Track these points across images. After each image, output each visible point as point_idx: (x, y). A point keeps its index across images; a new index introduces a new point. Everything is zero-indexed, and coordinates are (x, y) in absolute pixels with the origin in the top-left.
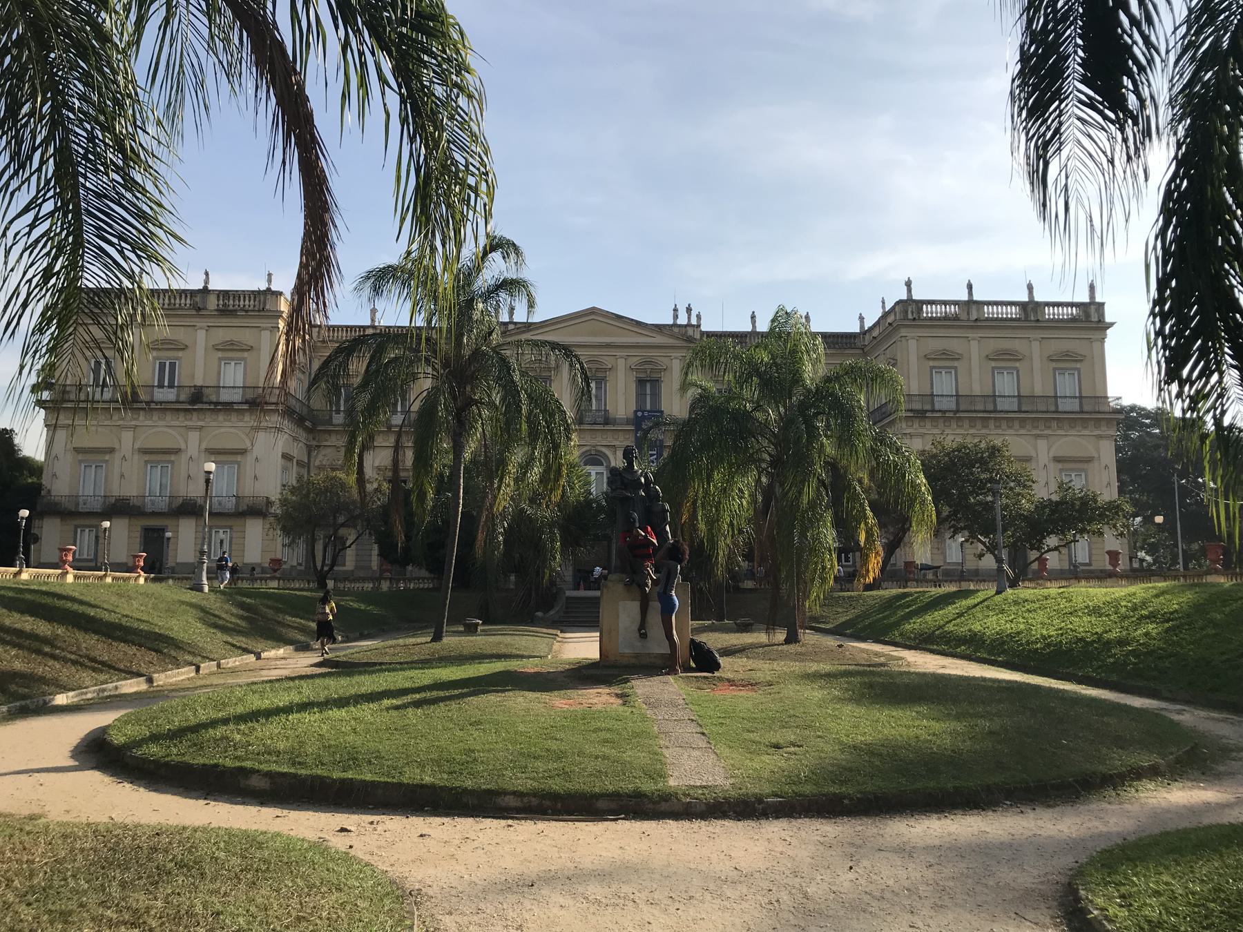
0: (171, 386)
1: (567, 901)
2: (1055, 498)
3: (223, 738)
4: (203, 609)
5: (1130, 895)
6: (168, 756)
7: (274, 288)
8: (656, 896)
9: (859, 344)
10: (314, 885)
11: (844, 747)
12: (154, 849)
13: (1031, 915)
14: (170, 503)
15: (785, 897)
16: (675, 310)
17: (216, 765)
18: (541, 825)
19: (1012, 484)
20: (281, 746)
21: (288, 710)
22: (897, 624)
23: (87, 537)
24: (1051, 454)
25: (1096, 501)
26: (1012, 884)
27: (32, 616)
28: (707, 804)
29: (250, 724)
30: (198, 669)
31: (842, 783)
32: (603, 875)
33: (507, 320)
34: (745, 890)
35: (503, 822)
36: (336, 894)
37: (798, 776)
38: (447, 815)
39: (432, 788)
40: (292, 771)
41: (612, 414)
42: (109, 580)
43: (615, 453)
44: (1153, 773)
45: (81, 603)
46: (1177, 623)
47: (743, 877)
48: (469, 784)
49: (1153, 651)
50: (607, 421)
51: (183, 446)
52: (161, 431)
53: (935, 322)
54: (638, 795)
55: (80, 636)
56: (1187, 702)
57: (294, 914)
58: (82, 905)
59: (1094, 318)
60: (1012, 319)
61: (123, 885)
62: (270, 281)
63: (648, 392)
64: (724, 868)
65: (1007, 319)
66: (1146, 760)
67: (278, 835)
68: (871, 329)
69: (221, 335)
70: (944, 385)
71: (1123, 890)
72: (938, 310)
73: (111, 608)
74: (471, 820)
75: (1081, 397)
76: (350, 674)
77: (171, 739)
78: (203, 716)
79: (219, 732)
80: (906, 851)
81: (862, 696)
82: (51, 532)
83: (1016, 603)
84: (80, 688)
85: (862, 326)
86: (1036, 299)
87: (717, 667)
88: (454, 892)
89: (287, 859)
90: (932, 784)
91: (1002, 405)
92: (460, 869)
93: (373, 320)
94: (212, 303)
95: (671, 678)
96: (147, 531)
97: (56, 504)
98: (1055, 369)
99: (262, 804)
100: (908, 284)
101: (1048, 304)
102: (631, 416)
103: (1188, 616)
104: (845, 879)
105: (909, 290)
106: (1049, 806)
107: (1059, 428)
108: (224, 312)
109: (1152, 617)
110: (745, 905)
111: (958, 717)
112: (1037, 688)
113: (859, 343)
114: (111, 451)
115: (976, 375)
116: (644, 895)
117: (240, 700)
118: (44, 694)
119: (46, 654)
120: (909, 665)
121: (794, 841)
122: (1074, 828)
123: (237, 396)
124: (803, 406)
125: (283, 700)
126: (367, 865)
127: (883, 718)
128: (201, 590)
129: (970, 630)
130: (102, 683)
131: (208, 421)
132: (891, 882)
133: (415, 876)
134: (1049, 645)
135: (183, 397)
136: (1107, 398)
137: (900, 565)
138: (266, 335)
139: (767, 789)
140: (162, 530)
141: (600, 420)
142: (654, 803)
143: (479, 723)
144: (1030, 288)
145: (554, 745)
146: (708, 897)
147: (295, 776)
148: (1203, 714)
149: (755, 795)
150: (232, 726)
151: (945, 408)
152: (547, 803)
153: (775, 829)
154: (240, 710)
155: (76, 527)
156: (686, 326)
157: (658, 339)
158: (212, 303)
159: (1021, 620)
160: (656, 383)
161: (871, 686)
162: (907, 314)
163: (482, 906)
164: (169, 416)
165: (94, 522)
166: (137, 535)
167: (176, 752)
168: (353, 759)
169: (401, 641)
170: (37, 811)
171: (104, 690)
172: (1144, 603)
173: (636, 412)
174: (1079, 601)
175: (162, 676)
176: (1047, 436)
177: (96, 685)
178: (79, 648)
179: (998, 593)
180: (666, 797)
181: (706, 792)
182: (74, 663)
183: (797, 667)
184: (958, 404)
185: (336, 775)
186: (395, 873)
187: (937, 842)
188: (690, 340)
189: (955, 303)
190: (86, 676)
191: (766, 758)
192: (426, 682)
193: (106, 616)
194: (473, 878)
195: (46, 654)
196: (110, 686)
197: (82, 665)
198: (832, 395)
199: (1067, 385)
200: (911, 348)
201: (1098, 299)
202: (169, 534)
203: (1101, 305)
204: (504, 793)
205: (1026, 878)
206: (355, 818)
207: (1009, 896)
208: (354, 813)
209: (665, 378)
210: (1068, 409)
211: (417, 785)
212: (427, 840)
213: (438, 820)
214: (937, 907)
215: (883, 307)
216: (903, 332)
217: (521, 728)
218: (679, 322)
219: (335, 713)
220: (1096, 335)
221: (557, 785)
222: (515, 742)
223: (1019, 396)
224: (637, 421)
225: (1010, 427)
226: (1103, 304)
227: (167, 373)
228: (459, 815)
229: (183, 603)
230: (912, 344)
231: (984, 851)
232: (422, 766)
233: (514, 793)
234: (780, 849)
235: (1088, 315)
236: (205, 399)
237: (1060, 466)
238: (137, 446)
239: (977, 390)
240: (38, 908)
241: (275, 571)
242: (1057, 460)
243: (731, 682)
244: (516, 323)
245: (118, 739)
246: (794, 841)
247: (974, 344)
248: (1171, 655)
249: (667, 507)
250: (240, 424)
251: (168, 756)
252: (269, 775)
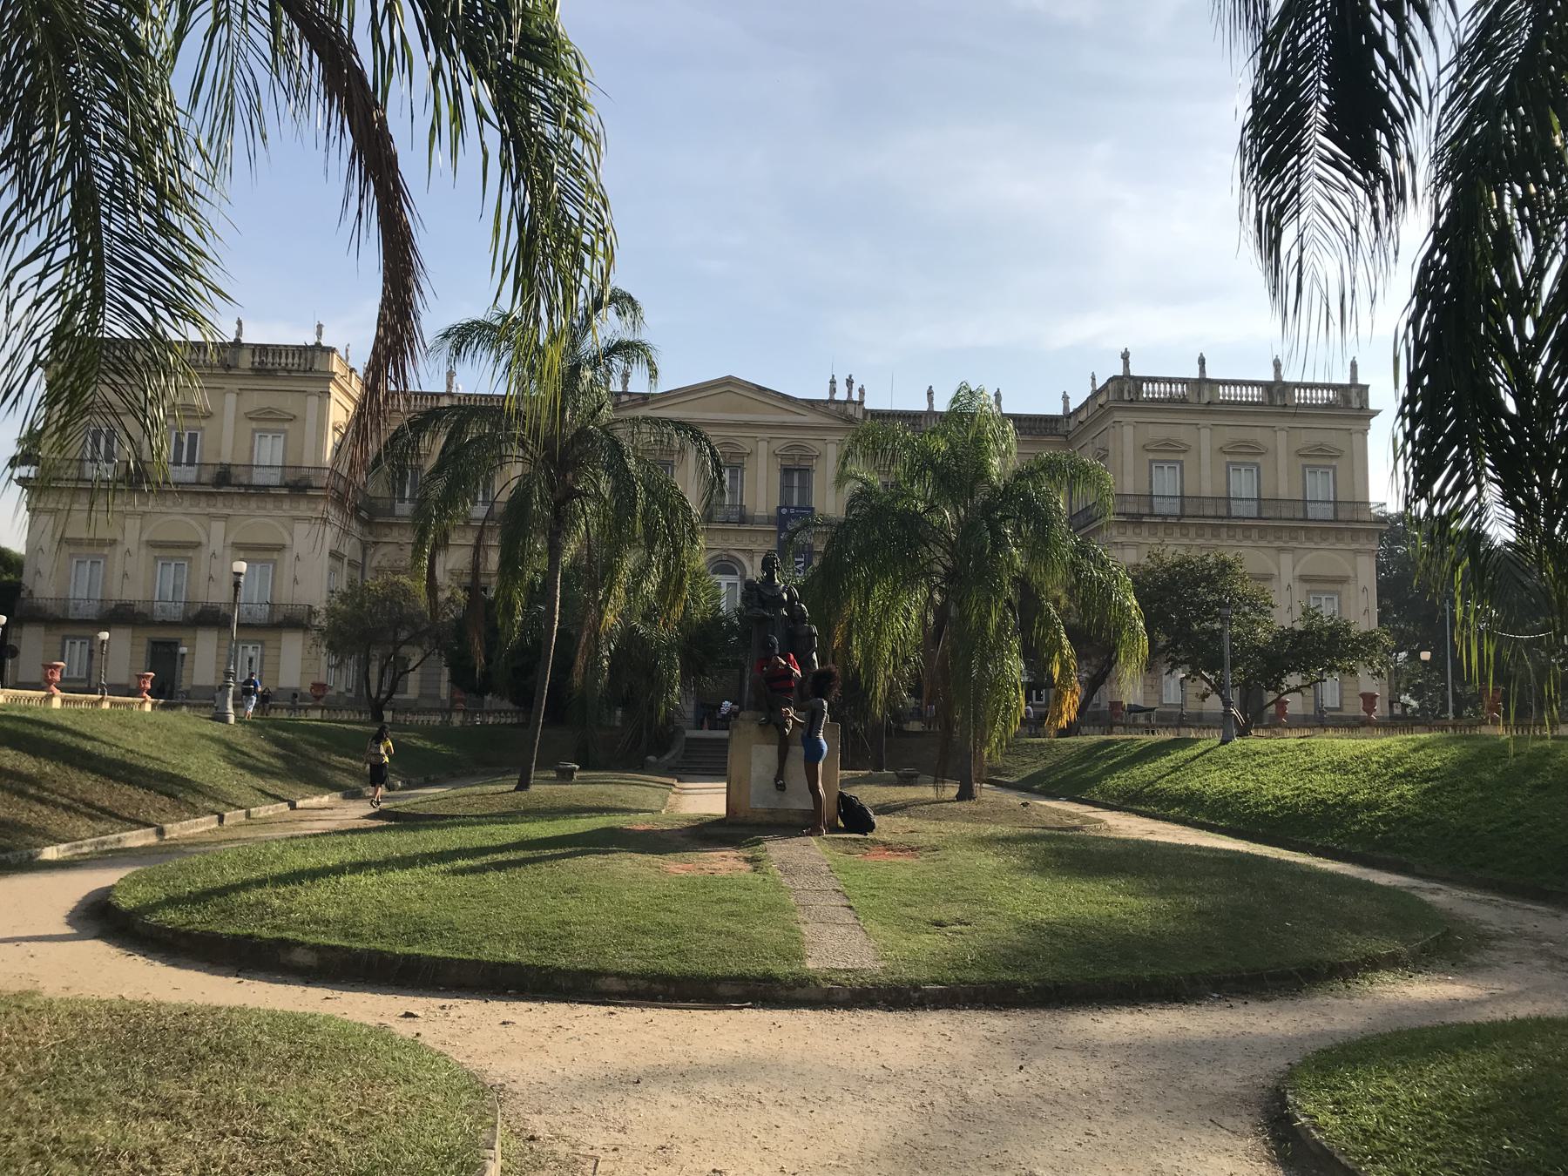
0: (191, 463)
1: (681, 1100)
2: (1299, 627)
3: (258, 903)
4: (228, 746)
5: (1346, 1101)
6: (189, 923)
7: (324, 343)
8: (787, 1096)
9: (1061, 430)
10: (378, 1076)
11: (1022, 927)
12: (184, 1031)
13: (1228, 1122)
14: (185, 612)
15: (940, 1099)
16: (833, 382)
17: (251, 936)
18: (650, 1013)
19: (1247, 609)
20: (331, 913)
21: (338, 870)
22: (1097, 779)
23: (77, 651)
24: (1298, 572)
25: (1348, 632)
26: (1211, 1088)
27: (13, 748)
28: (852, 991)
29: (291, 887)
30: (221, 819)
31: (1017, 968)
32: (723, 1072)
34: (893, 1091)
35: (604, 1009)
36: (404, 1087)
37: (964, 959)
38: (535, 1000)
39: (517, 966)
40: (345, 944)
41: (749, 510)
42: (106, 706)
43: (752, 559)
44: (1393, 963)
45: (75, 734)
46: (1438, 784)
47: (891, 1076)
48: (563, 962)
49: (1408, 817)
50: (743, 519)
51: (204, 540)
52: (177, 520)
53: (1156, 404)
54: (769, 979)
55: (74, 775)
56: (1444, 880)
57: (355, 1107)
58: (99, 1093)
59: (1356, 404)
60: (1252, 404)
61: (149, 1071)
62: (319, 334)
63: (796, 483)
64: (871, 1066)
65: (1247, 403)
66: (1383, 947)
67: (331, 1018)
68: (1077, 411)
69: (256, 401)
70: (1166, 483)
71: (1337, 1095)
72: (1161, 390)
73: (113, 741)
74: (564, 1006)
75: (1335, 502)
76: (415, 829)
77: (193, 903)
78: (232, 876)
79: (253, 896)
80: (1089, 1050)
81: (1048, 865)
82: (32, 644)
83: (1245, 755)
84: (74, 839)
85: (1066, 407)
86: (1286, 379)
87: (868, 826)
88: (543, 1088)
89: (344, 1046)
90: (1125, 972)
91: (1238, 509)
92: (551, 1062)
93: (449, 386)
94: (246, 360)
95: (813, 840)
96: (155, 645)
97: (39, 609)
98: (1304, 467)
99: (307, 983)
100: (1125, 357)
101: (1299, 385)
102: (773, 511)
103: (1452, 774)
104: (1013, 1081)
105: (1126, 364)
106: (1266, 1000)
107: (1309, 539)
108: (261, 372)
109: (1408, 776)
110: (892, 1108)
111: (1161, 893)
112: (1263, 859)
113: (1061, 429)
114: (113, 542)
115: (1206, 471)
116: (771, 1095)
117: (279, 857)
118: (29, 846)
119: (32, 797)
120: (1109, 829)
121: (955, 1037)
122: (1291, 1026)
123: (274, 478)
124: (988, 508)
125: (331, 859)
126: (440, 1054)
127: (1071, 893)
128: (225, 720)
129: (1187, 788)
130: (102, 834)
131: (238, 508)
132: (1067, 1085)
133: (497, 1070)
134: (1282, 808)
135: (205, 478)
136: (1368, 503)
137: (1105, 705)
138: (313, 401)
139: (925, 974)
140: (173, 645)
141: (735, 517)
142: (789, 989)
143: (575, 890)
144: (1277, 365)
145: (667, 918)
146: (848, 1097)
147: (348, 950)
148: (1464, 894)
149: (910, 981)
150: (269, 889)
151: (1165, 511)
152: (658, 987)
153: (932, 1022)
154: (278, 869)
155: (65, 638)
157: (810, 418)
158: (246, 360)
159: (1250, 777)
160: (805, 472)
161: (1058, 853)
162: (1123, 393)
163: (577, 1104)
164: (186, 503)
165: (88, 632)
166: (143, 650)
167: (200, 920)
168: (421, 931)
169: (477, 789)
170: (29, 987)
171: (104, 843)
172: (1399, 759)
173: (779, 508)
174: (1321, 756)
175: (177, 826)
176: (1293, 549)
177: (93, 836)
178: (72, 790)
179: (1224, 742)
180: (802, 982)
181: (851, 976)
182: (67, 808)
183: (969, 829)
184: (1182, 506)
185: (400, 949)
186: (473, 1065)
187: (1127, 1040)
188: (850, 420)
189: (1184, 381)
190: (82, 825)
191: (925, 938)
192: (510, 840)
193: (106, 751)
194: (567, 1073)
195: (32, 797)
196: (112, 837)
197: (76, 811)
198: (1024, 494)
199: (1319, 487)
200: (1127, 436)
201: (1361, 381)
202: (183, 650)
203: (1366, 387)
204: (604, 974)
205: (1231, 1080)
206: (422, 1001)
207: (1205, 1101)
208: (421, 995)
209: (817, 466)
210: (1320, 516)
211: (499, 964)
212: (510, 1028)
213: (525, 1005)
214: (1121, 1113)
215: (1093, 384)
216: (1117, 416)
217: (628, 896)
218: (837, 397)
219: (398, 876)
220: (1356, 426)
221: (670, 965)
222: (619, 914)
223: (1259, 499)
224: (781, 520)
225: (1248, 538)
226: (1366, 387)
227: (187, 450)
228: (551, 1000)
229: (202, 736)
230: (1128, 431)
231: (1182, 1050)
232: (505, 940)
233: (618, 974)
234: (937, 1045)
235: (1347, 401)
236: (233, 481)
237: (1308, 586)
238: (144, 538)
239: (1207, 491)
240: (48, 1096)
241: (318, 698)
242: (1304, 579)
243: (887, 846)
244: (630, 394)
245: (126, 902)
246: (955, 1037)
247: (1205, 433)
248: (1428, 823)
249: (815, 630)
250: (275, 513)
251: (189, 923)
252: (316, 948)
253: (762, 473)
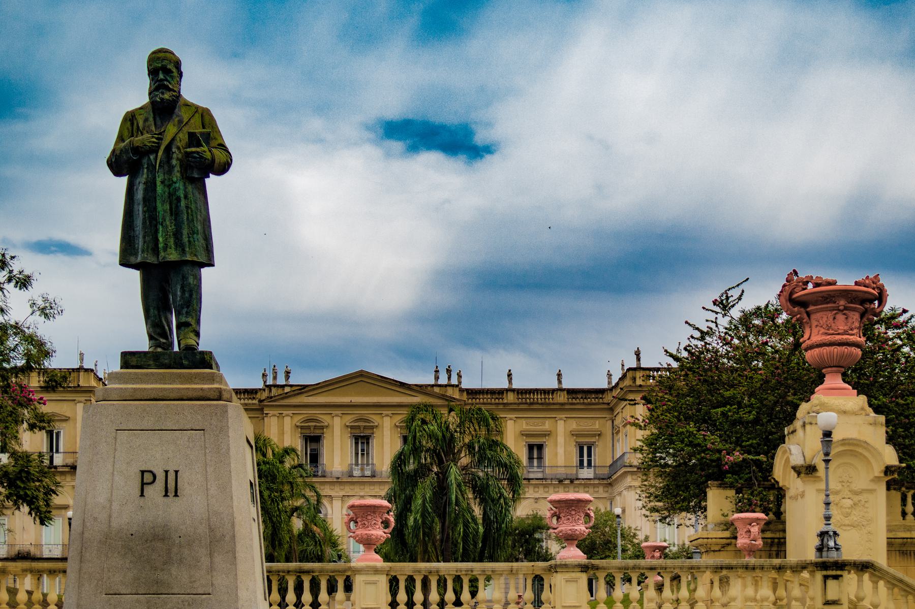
33: (284, 383)
62: (82, 360)
85: (609, 383)
156: (446, 386)
215: (623, 369)
218: (440, 382)
244: (291, 386)
253: (387, 440)
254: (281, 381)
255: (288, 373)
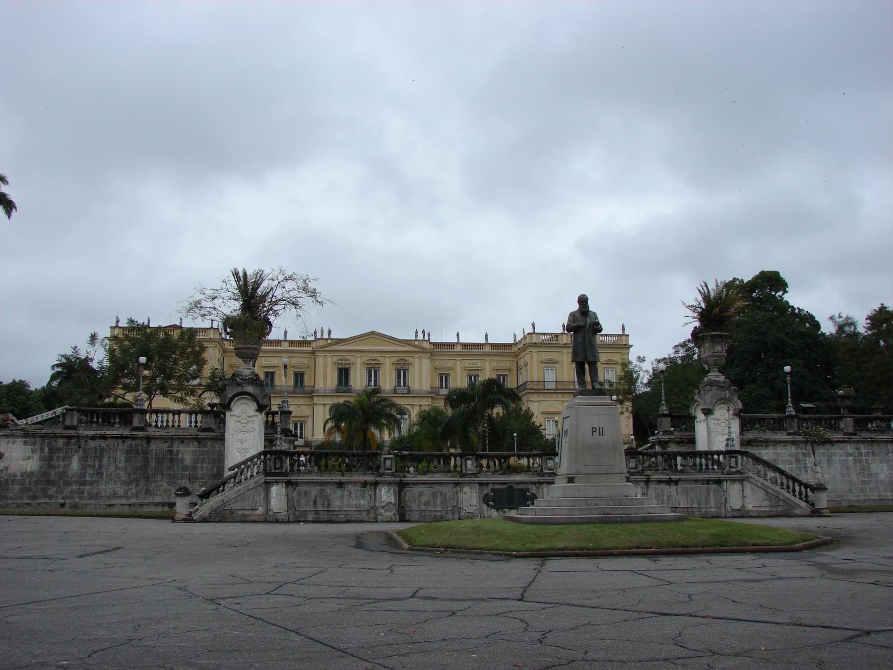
68: (520, 341)
70: (550, 376)
157: (407, 348)
200: (533, 359)
220: (624, 351)
230: (535, 355)
253: (388, 372)
254: (326, 336)
255: (330, 332)
